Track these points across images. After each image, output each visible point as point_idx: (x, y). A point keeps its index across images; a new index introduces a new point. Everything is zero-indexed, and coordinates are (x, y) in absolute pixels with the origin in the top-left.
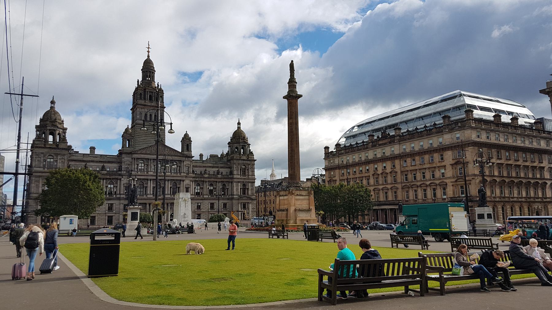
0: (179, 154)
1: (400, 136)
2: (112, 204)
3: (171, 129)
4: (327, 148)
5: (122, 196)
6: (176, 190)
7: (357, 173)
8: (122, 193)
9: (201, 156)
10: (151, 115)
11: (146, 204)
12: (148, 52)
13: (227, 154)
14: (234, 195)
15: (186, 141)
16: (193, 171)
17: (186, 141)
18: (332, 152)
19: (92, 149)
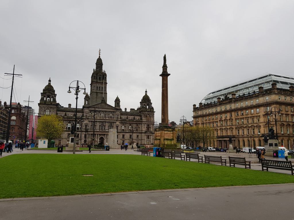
0: (113, 108)
1: (235, 99)
3: (85, 92)
4: (194, 105)
6: (111, 126)
7: (211, 119)
9: (126, 109)
10: (100, 87)
12: (100, 54)
13: (140, 108)
14: (142, 131)
15: (117, 101)
16: (121, 117)
17: (117, 101)
18: (198, 107)
19: (70, 105)
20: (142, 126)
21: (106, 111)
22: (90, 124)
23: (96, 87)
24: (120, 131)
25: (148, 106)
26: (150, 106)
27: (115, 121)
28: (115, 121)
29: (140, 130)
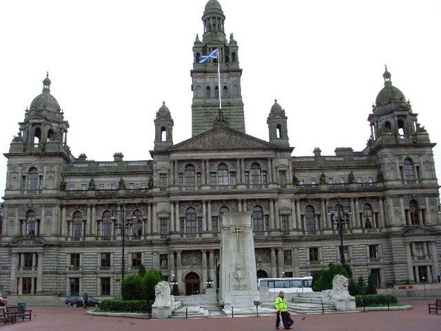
2: (139, 255)
5: (155, 237)
8: (155, 231)
11: (199, 252)
15: (277, 118)
16: (295, 180)
20: (385, 208)
21: (235, 160)
22: (176, 212)
23: (204, 88)
24: (295, 233)
25: (401, 131)
26: (412, 126)
28: (275, 196)
29: (382, 222)
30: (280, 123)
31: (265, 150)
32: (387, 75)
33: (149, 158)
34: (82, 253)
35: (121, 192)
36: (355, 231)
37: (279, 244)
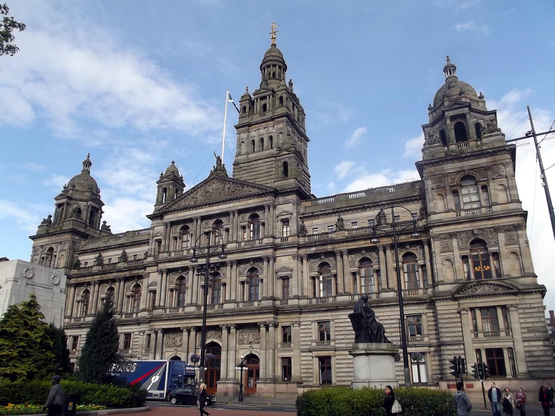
10: (262, 140)
24: (295, 302)
27: (270, 252)
28: (270, 252)
30: (287, 160)
31: (259, 195)
32: (450, 69)
33: (148, 223)
34: (81, 335)
35: (121, 265)
36: (384, 295)
37: (269, 318)
